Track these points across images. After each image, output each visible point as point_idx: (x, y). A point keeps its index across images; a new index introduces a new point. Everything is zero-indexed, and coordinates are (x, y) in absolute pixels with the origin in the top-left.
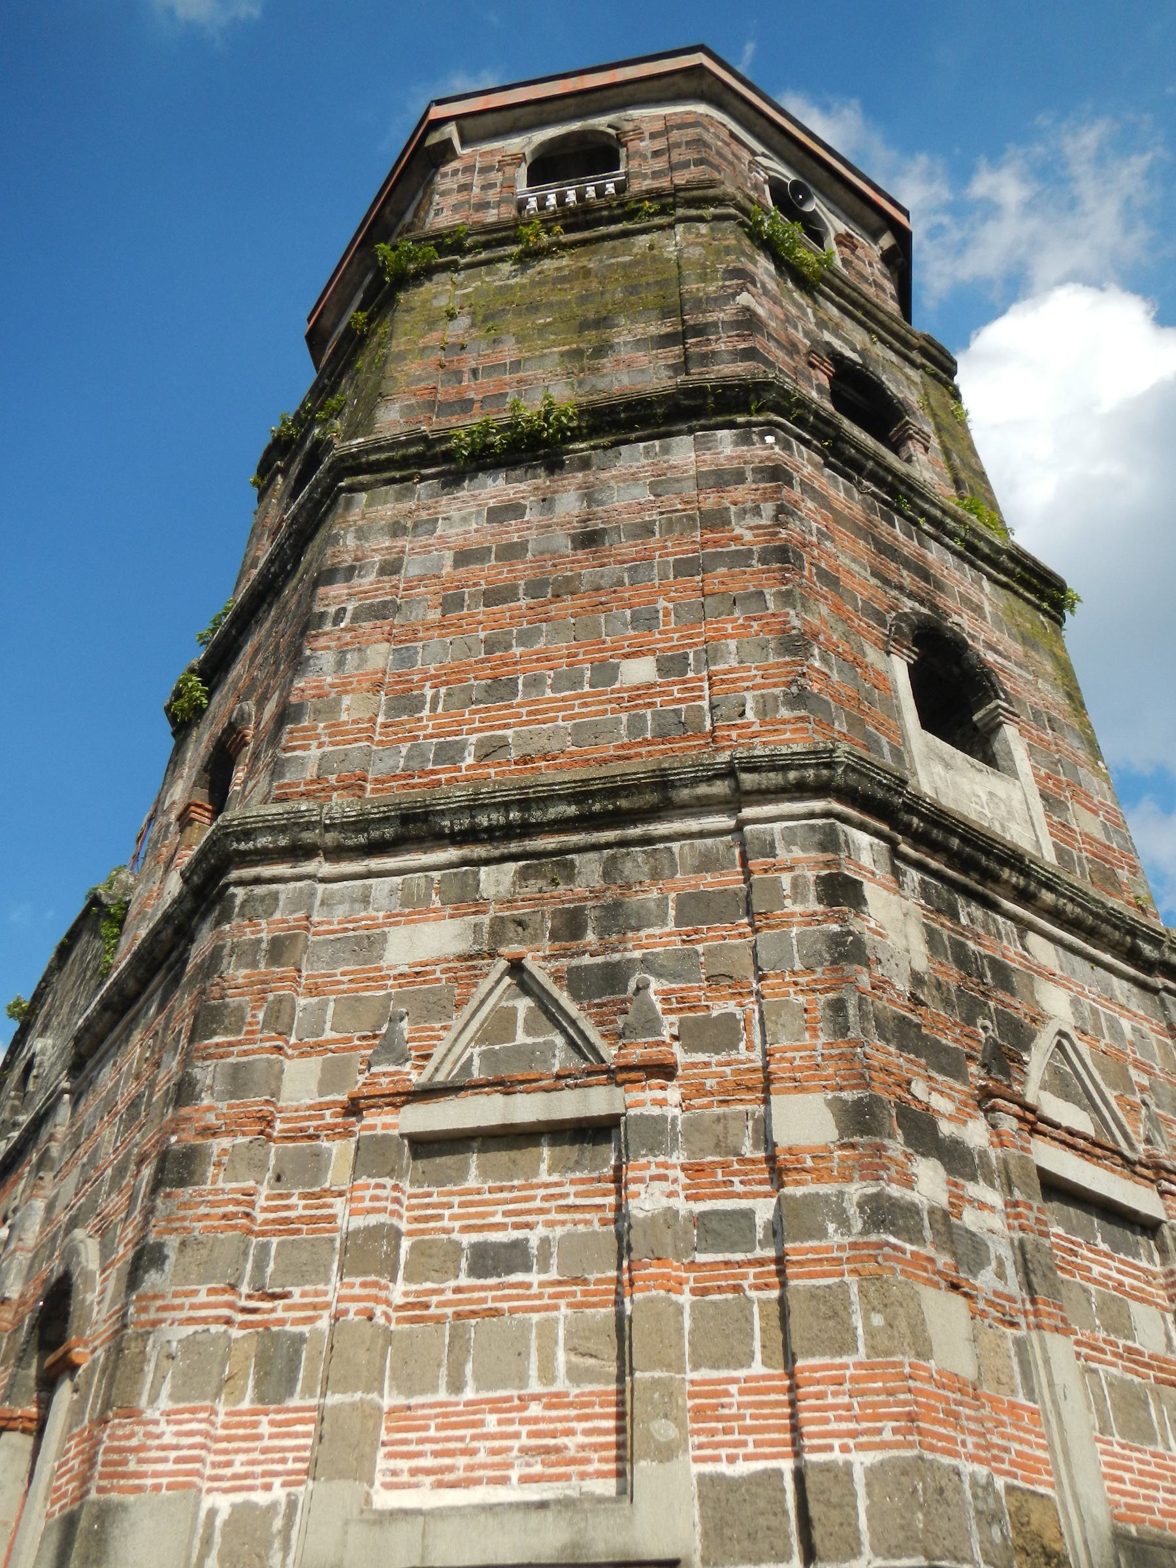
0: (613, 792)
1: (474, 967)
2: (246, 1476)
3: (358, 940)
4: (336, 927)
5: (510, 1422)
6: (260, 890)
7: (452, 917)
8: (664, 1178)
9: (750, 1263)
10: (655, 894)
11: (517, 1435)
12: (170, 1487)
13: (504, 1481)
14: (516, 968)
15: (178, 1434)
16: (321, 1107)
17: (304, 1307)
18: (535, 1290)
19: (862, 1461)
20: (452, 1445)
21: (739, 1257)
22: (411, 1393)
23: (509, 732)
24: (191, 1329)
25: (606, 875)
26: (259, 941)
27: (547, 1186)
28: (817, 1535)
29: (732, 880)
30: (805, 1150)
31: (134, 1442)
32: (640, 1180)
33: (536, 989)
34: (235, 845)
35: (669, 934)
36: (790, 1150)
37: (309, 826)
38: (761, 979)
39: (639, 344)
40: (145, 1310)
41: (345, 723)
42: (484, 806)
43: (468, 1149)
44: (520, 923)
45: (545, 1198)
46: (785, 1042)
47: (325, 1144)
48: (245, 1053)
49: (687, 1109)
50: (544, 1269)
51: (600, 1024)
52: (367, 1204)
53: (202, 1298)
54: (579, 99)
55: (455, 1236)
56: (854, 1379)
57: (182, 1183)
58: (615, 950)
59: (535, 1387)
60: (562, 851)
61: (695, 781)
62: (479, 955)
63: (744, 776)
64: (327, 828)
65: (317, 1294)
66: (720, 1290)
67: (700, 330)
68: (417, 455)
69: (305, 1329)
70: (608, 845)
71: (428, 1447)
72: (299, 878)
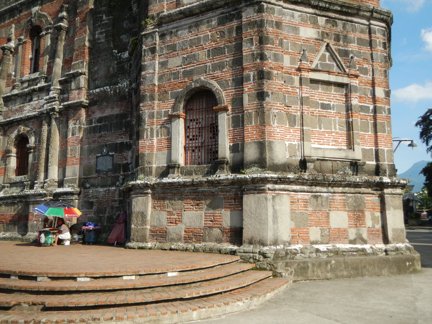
0: (348, 7)
1: (319, 43)
2: (290, 139)
3: (293, 27)
4: (287, 22)
5: (330, 135)
6: (270, 6)
7: (313, 28)
8: (357, 98)
9: (368, 116)
10: (353, 36)
11: (331, 138)
12: (280, 139)
13: (329, 145)
14: (328, 45)
15: (280, 130)
16: (291, 67)
17: (295, 110)
18: (332, 114)
19: (386, 149)
21: (367, 114)
22: (312, 128)
24: (278, 111)
25: (343, 27)
26: (273, 21)
27: (334, 94)
28: (380, 158)
29: (366, 37)
30: (380, 98)
31: (272, 131)
32: (353, 98)
33: (331, 51)
35: (356, 46)
36: (378, 98)
40: (268, 105)
43: (319, 84)
44: (327, 34)
45: (333, 97)
46: (377, 77)
47: (293, 76)
48: (276, 51)
49: (359, 85)
50: (334, 110)
51: (345, 63)
52: (305, 92)
53: (278, 105)
55: (318, 101)
56: (385, 137)
57: (269, 79)
58: (346, 47)
59: (333, 130)
60: (335, 18)
62: (319, 40)
65: (296, 108)
66: (364, 119)
69: (296, 114)
70: (344, 20)
71: (316, 138)
72: (279, 6)
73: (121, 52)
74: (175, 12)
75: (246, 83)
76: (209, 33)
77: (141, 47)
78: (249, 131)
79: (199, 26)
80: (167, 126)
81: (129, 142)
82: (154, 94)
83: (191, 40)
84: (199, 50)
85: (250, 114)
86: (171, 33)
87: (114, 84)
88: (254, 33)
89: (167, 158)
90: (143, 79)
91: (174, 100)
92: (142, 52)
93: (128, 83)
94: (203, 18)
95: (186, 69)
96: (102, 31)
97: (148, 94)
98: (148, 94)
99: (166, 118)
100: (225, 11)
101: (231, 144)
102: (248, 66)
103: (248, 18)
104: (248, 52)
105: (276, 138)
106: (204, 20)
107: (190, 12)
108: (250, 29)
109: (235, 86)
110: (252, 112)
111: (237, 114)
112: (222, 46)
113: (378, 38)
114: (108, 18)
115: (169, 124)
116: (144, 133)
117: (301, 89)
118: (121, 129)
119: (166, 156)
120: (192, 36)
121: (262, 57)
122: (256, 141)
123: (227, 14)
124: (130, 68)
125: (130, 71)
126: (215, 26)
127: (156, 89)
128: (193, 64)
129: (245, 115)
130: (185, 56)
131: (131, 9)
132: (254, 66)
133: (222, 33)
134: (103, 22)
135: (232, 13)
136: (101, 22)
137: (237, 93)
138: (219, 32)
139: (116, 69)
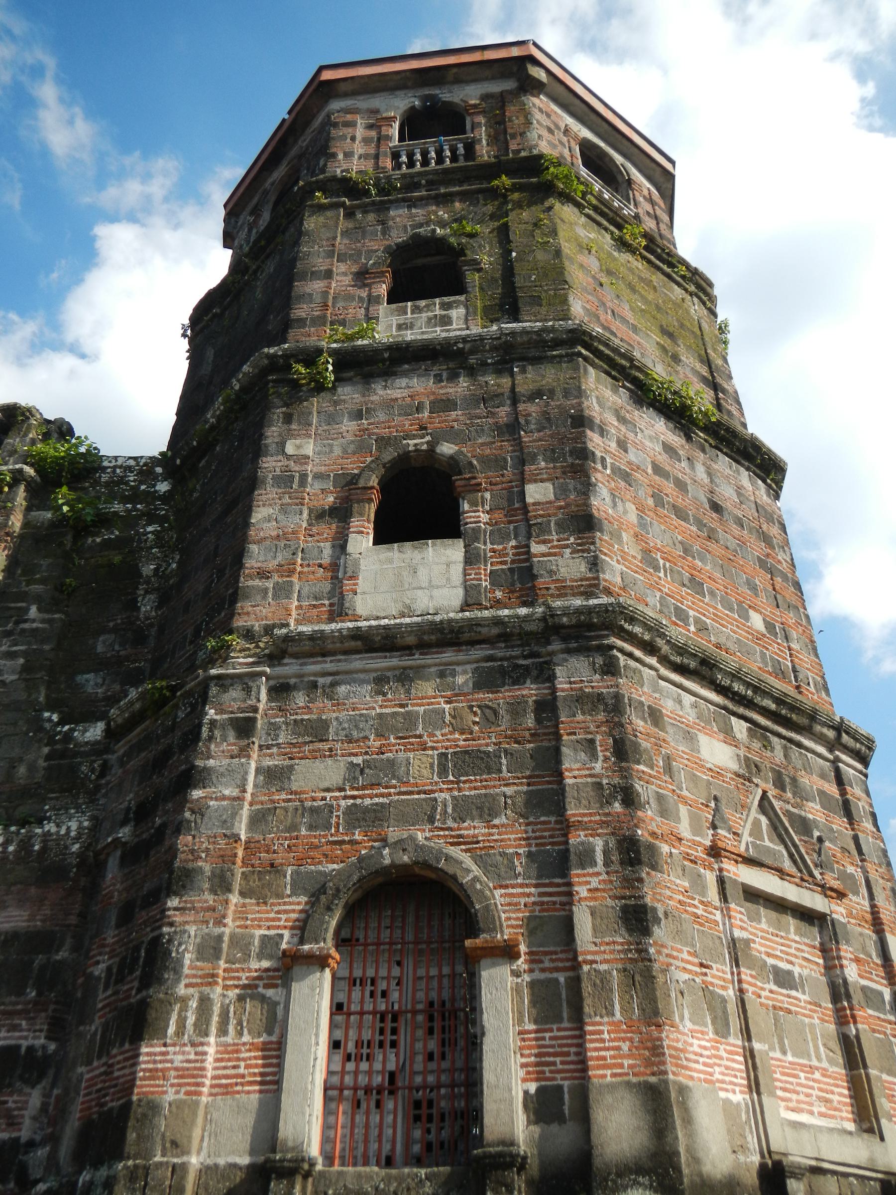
6: (632, 663)
15: (700, 1046)
18: (802, 1004)
20: (788, 1086)
23: (708, 621)
25: (785, 756)
26: (641, 703)
29: (832, 790)
32: (846, 958)
34: (623, 622)
37: (663, 635)
38: (862, 860)
39: (693, 370)
41: (628, 554)
42: (740, 678)
44: (756, 766)
47: (702, 870)
50: (804, 993)
51: (807, 853)
54: (610, 129)
55: (763, 956)
59: (815, 1063)
61: (824, 724)
63: (845, 736)
64: (668, 642)
67: (724, 391)
68: (623, 368)
70: (784, 738)
73: (77, 723)
74: (340, 631)
75: (579, 871)
76: (447, 707)
77: (204, 713)
78: (603, 1041)
79: (412, 680)
80: (270, 993)
81: (44, 1047)
82: (231, 871)
83: (380, 716)
84: (410, 750)
85: (604, 977)
86: (314, 685)
87: (23, 823)
88: (598, 727)
89: (255, 1128)
90: (193, 812)
91: (303, 899)
92: (200, 725)
93: (86, 824)
94: (429, 662)
95: (359, 801)
96: (15, 648)
97: (207, 868)
98: (207, 868)
99: (266, 964)
100: (499, 653)
101: (532, 1087)
102: (586, 819)
103: (574, 683)
104: (581, 776)
105: (695, 1075)
106: (429, 666)
107: (386, 637)
108: (583, 713)
109: (539, 877)
110: (609, 972)
111: (547, 975)
112: (490, 749)
113: (859, 800)
114: (46, 616)
115: (275, 986)
116: (169, 1014)
117: (727, 914)
118: (21, 992)
119: (249, 1120)
120: (386, 707)
121: (629, 798)
122: (634, 1080)
123: (505, 664)
124: (102, 775)
125: (98, 788)
126: (466, 690)
127: (240, 853)
128: (387, 787)
129: (584, 978)
130: (358, 760)
131: (133, 606)
132: (604, 822)
133: (487, 711)
134: (26, 626)
135: (521, 662)
136: (17, 623)
137: (546, 899)
138: (479, 707)
139: (39, 776)
